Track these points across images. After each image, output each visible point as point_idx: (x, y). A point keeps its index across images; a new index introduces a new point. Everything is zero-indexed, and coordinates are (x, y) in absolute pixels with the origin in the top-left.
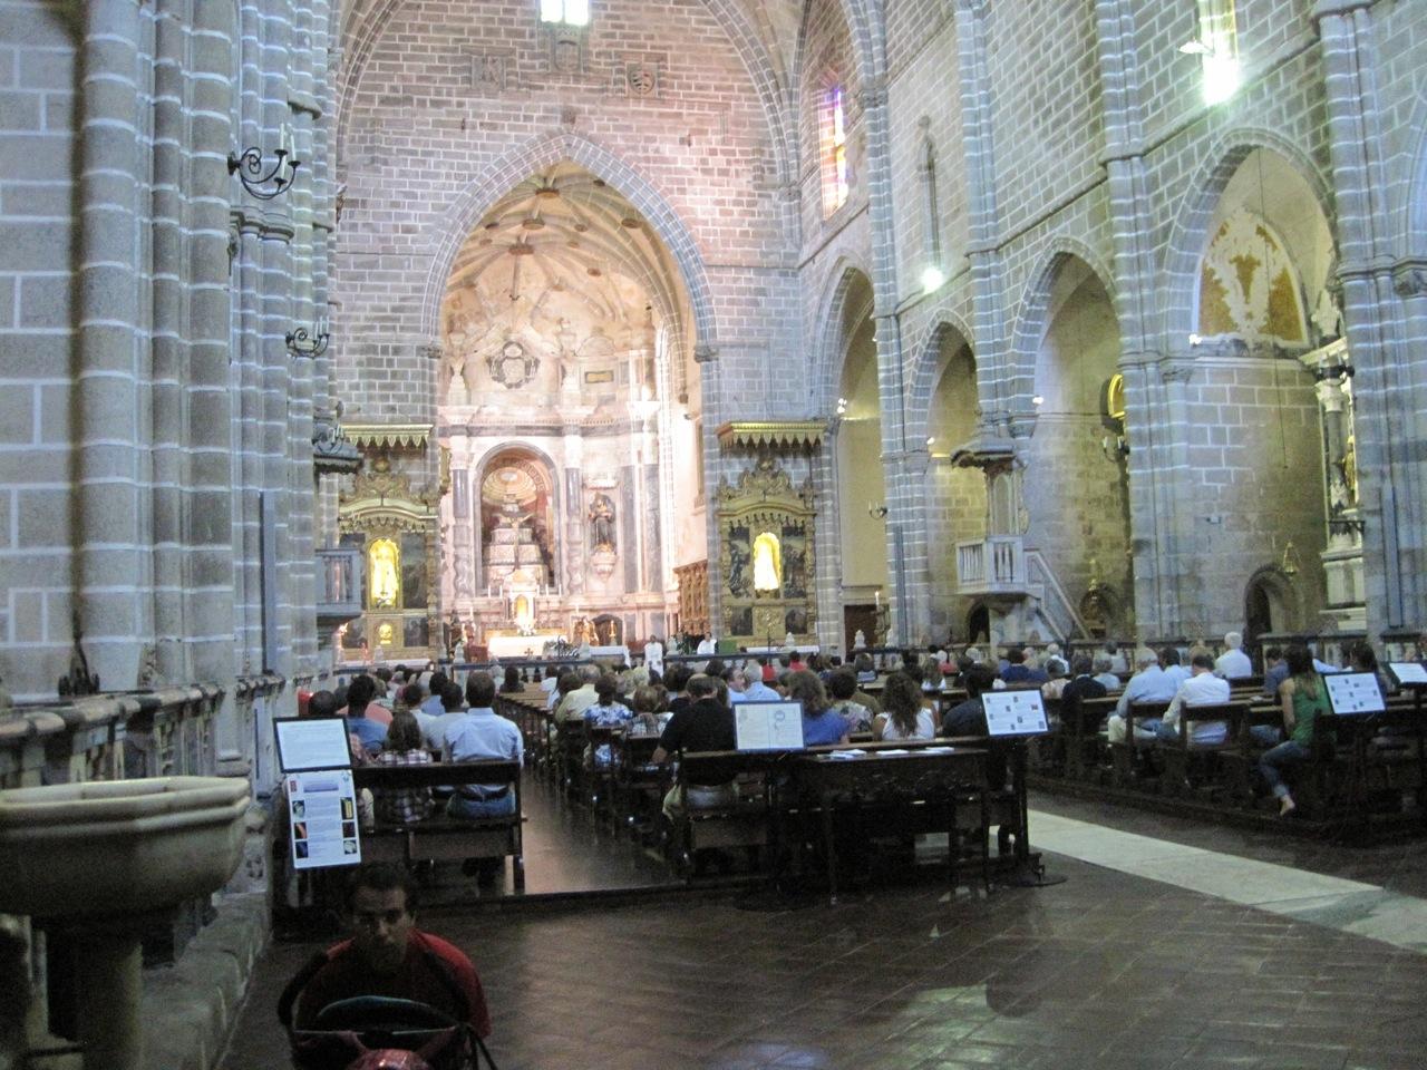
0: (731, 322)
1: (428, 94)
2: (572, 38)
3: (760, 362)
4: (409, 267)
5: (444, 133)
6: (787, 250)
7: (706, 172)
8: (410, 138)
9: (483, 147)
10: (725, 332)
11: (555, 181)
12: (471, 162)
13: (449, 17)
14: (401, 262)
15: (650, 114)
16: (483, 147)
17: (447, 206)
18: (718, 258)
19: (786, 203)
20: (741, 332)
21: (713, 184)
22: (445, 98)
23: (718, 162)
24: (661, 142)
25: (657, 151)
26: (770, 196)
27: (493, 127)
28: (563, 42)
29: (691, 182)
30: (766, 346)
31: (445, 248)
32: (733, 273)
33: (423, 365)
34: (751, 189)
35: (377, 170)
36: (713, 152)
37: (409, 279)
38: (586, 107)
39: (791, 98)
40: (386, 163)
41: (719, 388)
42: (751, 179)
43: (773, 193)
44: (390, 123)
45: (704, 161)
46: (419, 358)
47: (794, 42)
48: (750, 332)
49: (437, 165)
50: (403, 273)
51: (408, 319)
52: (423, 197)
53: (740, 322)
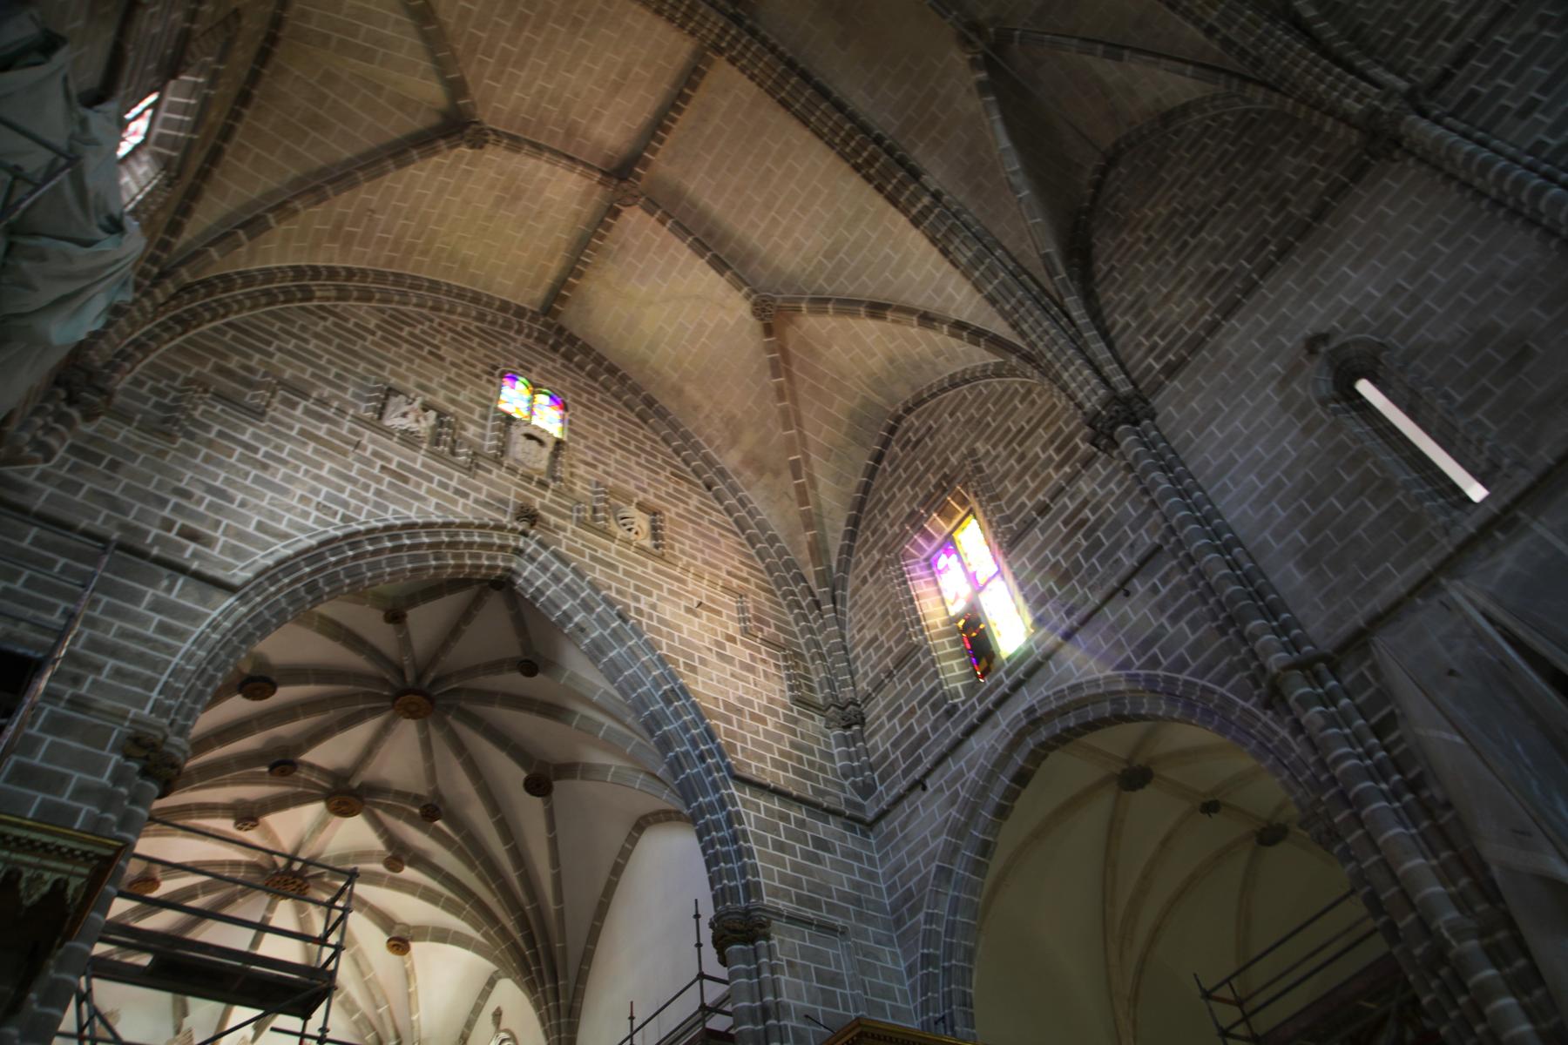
0: (783, 878)
1: (306, 396)
2: (543, 437)
3: (838, 965)
4: (169, 589)
5: (316, 451)
6: (848, 796)
7: (721, 657)
8: (251, 430)
9: (379, 493)
10: (775, 893)
11: (435, 682)
12: (353, 502)
13: (365, 348)
14: (159, 578)
15: (644, 565)
16: (379, 493)
17: (286, 536)
18: (753, 770)
19: (838, 732)
20: (801, 900)
21: (733, 675)
22: (330, 413)
23: (740, 652)
24: (660, 598)
25: (653, 607)
26: (812, 718)
27: (406, 480)
28: (530, 437)
29: (703, 661)
30: (843, 932)
31: (259, 588)
32: (776, 805)
33: (119, 777)
34: (788, 701)
35: (170, 437)
36: (732, 639)
37: (157, 606)
38: (553, 519)
39: (834, 603)
40: (191, 436)
41: (776, 994)
42: (785, 688)
43: (817, 717)
44: (220, 396)
45: (719, 645)
46: (116, 758)
47: (840, 536)
48: (815, 905)
49: (289, 479)
50: (150, 593)
51: (118, 673)
52: (243, 504)
53: (796, 883)
